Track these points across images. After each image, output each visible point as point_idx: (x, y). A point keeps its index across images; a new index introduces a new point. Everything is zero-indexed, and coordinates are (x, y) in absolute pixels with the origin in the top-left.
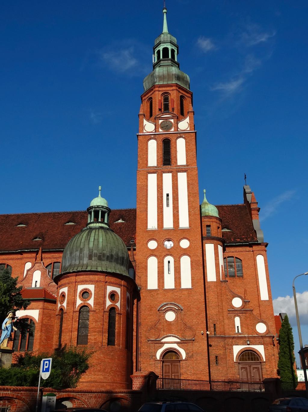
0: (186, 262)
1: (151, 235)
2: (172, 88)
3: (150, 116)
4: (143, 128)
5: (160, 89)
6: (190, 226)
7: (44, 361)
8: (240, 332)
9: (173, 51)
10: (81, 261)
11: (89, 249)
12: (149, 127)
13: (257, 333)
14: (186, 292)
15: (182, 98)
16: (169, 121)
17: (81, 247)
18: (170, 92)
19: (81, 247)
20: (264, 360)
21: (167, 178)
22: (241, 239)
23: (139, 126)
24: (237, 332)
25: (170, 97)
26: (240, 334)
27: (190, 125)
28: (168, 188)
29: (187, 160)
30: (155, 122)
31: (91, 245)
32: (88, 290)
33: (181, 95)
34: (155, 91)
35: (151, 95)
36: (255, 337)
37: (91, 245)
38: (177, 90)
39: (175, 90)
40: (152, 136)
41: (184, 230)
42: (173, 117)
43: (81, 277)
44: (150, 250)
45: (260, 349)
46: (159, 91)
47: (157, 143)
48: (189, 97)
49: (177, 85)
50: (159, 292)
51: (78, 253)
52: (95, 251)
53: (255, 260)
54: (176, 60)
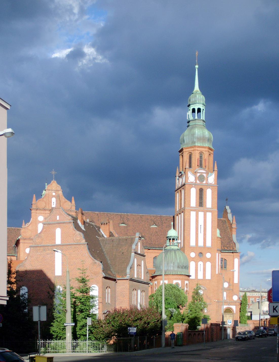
0: (209, 265)
1: (193, 249)
5: (198, 149)
6: (212, 246)
7: (229, 321)
8: (226, 299)
10: (174, 269)
11: (178, 263)
13: (233, 300)
14: (208, 281)
17: (174, 261)
19: (174, 261)
20: (235, 313)
22: (227, 248)
24: (224, 299)
25: (203, 155)
26: (226, 300)
27: (215, 180)
28: (201, 222)
29: (212, 205)
30: (195, 175)
31: (178, 261)
32: (178, 283)
34: (195, 150)
35: (192, 151)
36: (232, 302)
37: (178, 261)
40: (194, 186)
41: (209, 248)
42: (206, 173)
43: (175, 277)
44: (192, 258)
45: (234, 308)
46: (198, 150)
47: (196, 191)
50: (195, 280)
51: (172, 265)
52: (180, 264)
53: (234, 261)
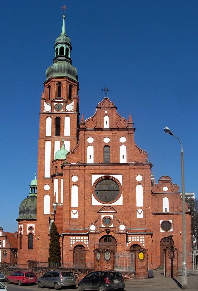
2: (63, 80)
3: (49, 100)
4: (43, 108)
9: (67, 49)
12: (47, 108)
15: (70, 87)
16: (61, 104)
18: (62, 82)
21: (57, 144)
23: (42, 107)
27: (74, 107)
33: (70, 84)
34: (52, 81)
35: (50, 84)
38: (67, 81)
39: (65, 81)
46: (55, 81)
48: (75, 85)
49: (67, 77)
54: (69, 56)
